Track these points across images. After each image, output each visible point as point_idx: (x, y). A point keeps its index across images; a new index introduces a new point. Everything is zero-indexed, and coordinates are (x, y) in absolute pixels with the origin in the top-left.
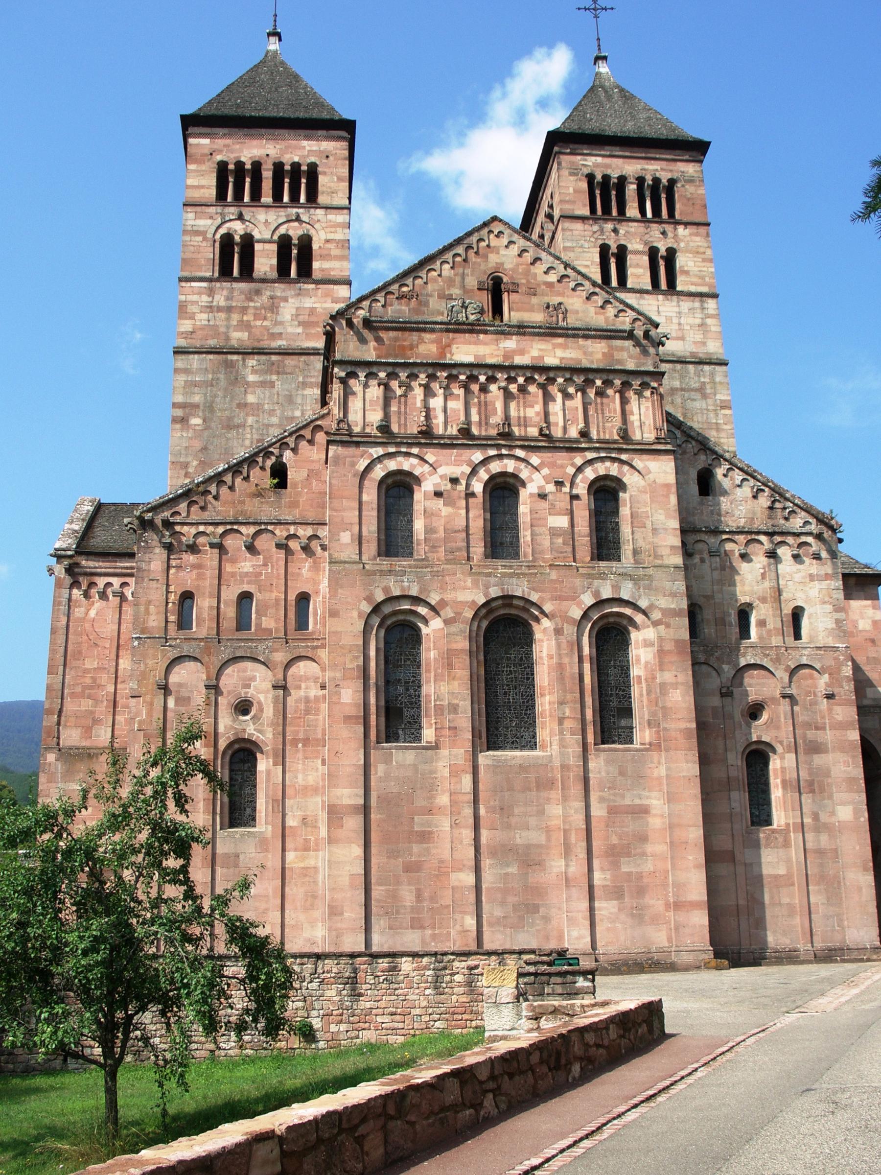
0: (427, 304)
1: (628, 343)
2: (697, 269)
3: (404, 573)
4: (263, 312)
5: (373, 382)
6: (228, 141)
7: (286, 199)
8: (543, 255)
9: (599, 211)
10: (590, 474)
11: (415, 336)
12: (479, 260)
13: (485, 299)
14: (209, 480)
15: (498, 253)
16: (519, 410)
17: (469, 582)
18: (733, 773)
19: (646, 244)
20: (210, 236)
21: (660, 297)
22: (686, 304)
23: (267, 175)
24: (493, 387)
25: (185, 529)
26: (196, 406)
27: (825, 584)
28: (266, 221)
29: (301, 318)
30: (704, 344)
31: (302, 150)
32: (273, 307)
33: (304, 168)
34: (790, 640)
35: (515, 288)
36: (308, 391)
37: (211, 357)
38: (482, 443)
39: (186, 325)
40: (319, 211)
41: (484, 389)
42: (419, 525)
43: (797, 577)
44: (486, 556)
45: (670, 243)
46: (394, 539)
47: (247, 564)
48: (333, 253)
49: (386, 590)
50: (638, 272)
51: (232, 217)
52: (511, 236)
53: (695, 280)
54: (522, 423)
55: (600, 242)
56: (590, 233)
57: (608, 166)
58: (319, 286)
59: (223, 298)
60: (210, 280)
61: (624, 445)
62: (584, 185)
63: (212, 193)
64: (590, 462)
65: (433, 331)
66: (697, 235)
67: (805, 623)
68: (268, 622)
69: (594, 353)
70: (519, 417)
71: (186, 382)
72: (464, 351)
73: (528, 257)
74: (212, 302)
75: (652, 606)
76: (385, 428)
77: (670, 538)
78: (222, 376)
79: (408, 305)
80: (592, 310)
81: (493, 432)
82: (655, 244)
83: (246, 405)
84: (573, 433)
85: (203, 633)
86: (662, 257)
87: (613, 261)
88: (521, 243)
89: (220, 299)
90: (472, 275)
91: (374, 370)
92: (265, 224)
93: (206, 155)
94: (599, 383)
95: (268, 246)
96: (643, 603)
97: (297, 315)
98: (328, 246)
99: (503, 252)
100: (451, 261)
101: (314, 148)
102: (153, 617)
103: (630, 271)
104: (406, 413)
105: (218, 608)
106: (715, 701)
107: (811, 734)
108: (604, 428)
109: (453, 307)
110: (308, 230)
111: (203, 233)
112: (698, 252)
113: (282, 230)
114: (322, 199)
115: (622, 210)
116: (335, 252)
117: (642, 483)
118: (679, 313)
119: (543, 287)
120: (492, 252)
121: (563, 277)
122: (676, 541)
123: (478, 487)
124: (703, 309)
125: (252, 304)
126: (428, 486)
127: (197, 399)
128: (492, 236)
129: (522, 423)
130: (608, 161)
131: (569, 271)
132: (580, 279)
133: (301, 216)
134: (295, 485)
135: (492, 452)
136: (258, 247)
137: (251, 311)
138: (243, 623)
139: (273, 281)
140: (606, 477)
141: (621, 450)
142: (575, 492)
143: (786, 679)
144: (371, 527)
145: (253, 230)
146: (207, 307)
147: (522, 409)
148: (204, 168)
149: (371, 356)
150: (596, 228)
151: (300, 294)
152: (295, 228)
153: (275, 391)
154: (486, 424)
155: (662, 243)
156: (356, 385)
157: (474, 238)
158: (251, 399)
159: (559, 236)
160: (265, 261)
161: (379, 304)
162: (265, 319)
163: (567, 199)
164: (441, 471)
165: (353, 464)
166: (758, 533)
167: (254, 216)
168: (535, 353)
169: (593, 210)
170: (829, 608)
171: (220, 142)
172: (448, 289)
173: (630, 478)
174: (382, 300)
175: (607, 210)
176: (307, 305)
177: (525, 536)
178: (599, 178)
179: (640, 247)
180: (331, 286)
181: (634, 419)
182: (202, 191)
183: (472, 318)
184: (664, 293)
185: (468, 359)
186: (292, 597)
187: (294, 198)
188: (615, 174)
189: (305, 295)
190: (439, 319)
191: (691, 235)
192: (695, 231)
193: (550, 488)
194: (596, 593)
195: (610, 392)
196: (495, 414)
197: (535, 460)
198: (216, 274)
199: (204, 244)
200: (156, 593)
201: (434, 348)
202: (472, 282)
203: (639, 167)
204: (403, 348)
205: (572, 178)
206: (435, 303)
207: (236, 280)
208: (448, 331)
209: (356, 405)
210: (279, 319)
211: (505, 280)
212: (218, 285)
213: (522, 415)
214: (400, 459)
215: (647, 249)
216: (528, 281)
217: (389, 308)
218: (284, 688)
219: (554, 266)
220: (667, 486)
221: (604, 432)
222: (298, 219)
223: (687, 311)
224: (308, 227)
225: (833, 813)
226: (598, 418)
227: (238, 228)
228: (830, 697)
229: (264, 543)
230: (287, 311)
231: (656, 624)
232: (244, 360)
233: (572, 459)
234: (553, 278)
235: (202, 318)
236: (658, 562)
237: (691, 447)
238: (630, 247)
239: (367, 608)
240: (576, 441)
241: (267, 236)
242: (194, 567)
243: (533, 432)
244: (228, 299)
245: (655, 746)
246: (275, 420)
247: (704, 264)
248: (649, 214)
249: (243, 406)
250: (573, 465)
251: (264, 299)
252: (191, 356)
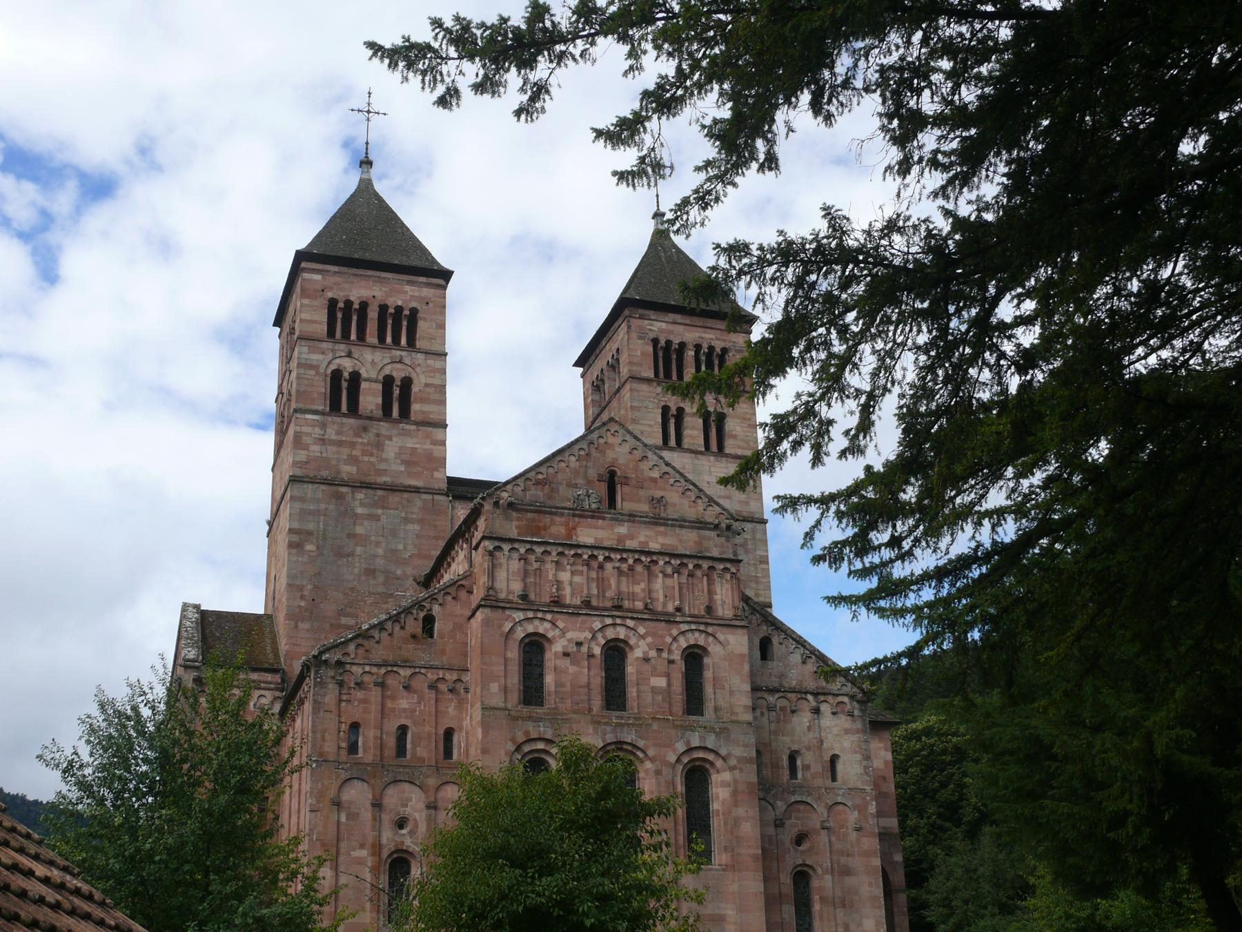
0: (557, 492)
1: (713, 534)
3: (541, 720)
5: (515, 555)
6: (337, 279)
7: (389, 340)
8: (650, 454)
10: (683, 643)
11: (547, 519)
13: (603, 487)
14: (373, 627)
17: (591, 730)
18: (784, 890)
20: (322, 370)
21: (712, 458)
23: (373, 314)
24: (609, 566)
25: (354, 669)
26: (310, 533)
27: (855, 738)
29: (403, 457)
30: (747, 503)
31: (405, 294)
32: (379, 445)
33: (407, 312)
34: (828, 782)
36: (410, 527)
37: (323, 487)
38: (600, 611)
39: (302, 456)
41: (601, 567)
42: (549, 679)
43: (835, 731)
44: (602, 708)
46: (532, 692)
47: (404, 703)
48: (431, 397)
49: (527, 733)
57: (671, 332)
60: (322, 413)
61: (708, 618)
62: (651, 349)
63: (323, 328)
64: (683, 633)
65: (562, 515)
67: (840, 767)
68: (421, 752)
69: (686, 541)
71: (301, 509)
72: (586, 535)
73: (638, 454)
75: (729, 754)
76: (524, 597)
77: (743, 699)
78: (332, 507)
81: (609, 604)
83: (355, 535)
84: (670, 608)
85: (369, 758)
91: (516, 546)
92: (371, 363)
93: (316, 291)
94: (691, 566)
96: (723, 752)
97: (400, 454)
98: (428, 390)
99: (617, 449)
101: (416, 294)
102: (327, 744)
103: (686, 432)
105: (381, 738)
106: (771, 830)
107: (843, 860)
111: (314, 367)
113: (387, 371)
116: (434, 396)
117: (723, 652)
122: (748, 702)
123: (597, 651)
125: (360, 440)
126: (558, 647)
127: (311, 526)
130: (671, 327)
131: (668, 469)
134: (441, 636)
135: (609, 621)
136: (364, 385)
137: (358, 447)
138: (401, 750)
139: (379, 420)
140: (696, 646)
141: (707, 624)
142: (672, 657)
143: (826, 814)
144: (515, 680)
148: (316, 303)
149: (514, 534)
151: (406, 434)
153: (380, 523)
154: (604, 596)
156: (501, 557)
158: (359, 530)
159: (626, 393)
160: (370, 399)
162: (372, 455)
164: (569, 635)
165: (501, 626)
166: (806, 693)
168: (642, 539)
170: (859, 757)
171: (331, 280)
173: (714, 648)
176: (410, 445)
177: (632, 692)
178: (662, 343)
181: (718, 597)
182: (315, 326)
183: (594, 506)
184: (714, 455)
185: (589, 541)
186: (441, 732)
187: (396, 341)
188: (676, 341)
190: (568, 504)
193: (653, 654)
194: (688, 742)
195: (699, 573)
197: (642, 630)
199: (317, 378)
200: (330, 722)
201: (563, 530)
202: (592, 473)
203: (697, 335)
204: (539, 528)
205: (640, 342)
206: (563, 491)
207: (345, 415)
208: (574, 515)
209: (501, 575)
210: (384, 455)
212: (330, 419)
214: (536, 622)
218: (435, 808)
220: (742, 655)
225: (860, 925)
227: (347, 365)
228: (858, 830)
229: (420, 684)
230: (390, 450)
231: (732, 769)
232: (353, 493)
233: (670, 630)
235: (315, 449)
236: (734, 718)
237: (756, 618)
239: (511, 747)
240: (673, 615)
241: (373, 375)
242: (360, 701)
243: (639, 605)
244: (338, 433)
245: (726, 868)
246: (380, 551)
249: (352, 536)
250: (670, 635)
252: (306, 486)
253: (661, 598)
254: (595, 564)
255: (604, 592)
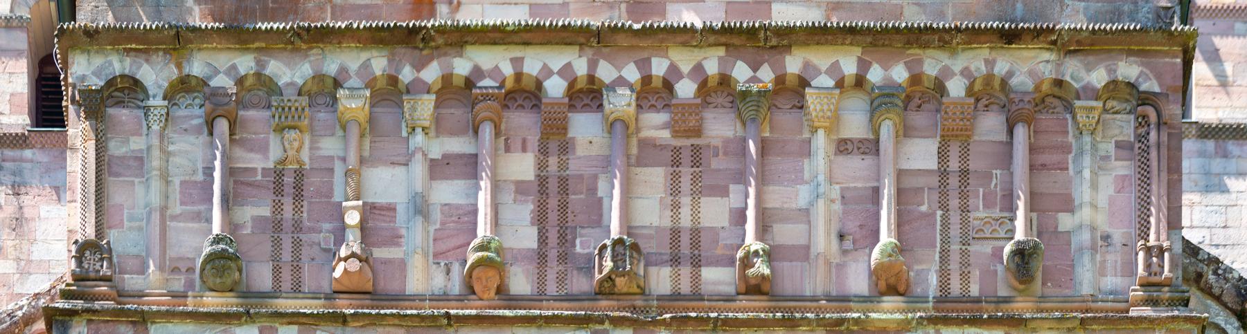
16: (676, 207)
54: (685, 249)
70: (675, 233)
104: (298, 227)
108: (965, 263)
129: (685, 249)
147: (686, 201)
196: (598, 219)
213: (686, 220)
221: (965, 277)
226: (946, 225)
253: (823, 242)
254: (523, 122)
255: (565, 240)
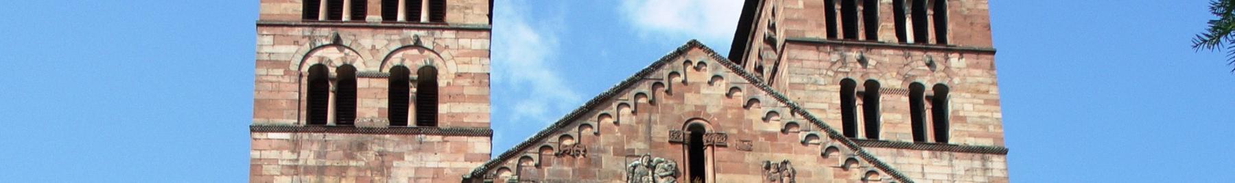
0: (598, 163)
2: (976, 114)
4: (369, 173)
7: (401, 16)
8: (762, 95)
9: (840, 34)
12: (671, 102)
13: (680, 156)
15: (698, 92)
19: (905, 79)
20: (294, 68)
21: (926, 153)
22: (962, 163)
28: (373, 47)
35: (721, 142)
40: (447, 34)
45: (940, 78)
48: (466, 92)
50: (895, 119)
51: (326, 42)
52: (716, 68)
53: (974, 129)
55: (842, 77)
56: (827, 65)
58: (447, 138)
59: (312, 155)
60: (294, 129)
66: (977, 66)
73: (740, 97)
74: (297, 160)
79: (572, 164)
80: (830, 171)
82: (918, 80)
86: (928, 98)
87: (859, 103)
88: (731, 77)
89: (308, 157)
90: (661, 122)
95: (375, 83)
98: (460, 82)
99: (705, 90)
100: (632, 103)
109: (635, 167)
110: (432, 61)
111: (284, 65)
112: (978, 91)
113: (396, 60)
114: (451, 17)
115: (871, 33)
116: (470, 90)
118: (953, 175)
119: (761, 139)
120: (690, 91)
121: (790, 125)
124: (985, 169)
125: (352, 163)
128: (689, 68)
131: (798, 118)
132: (813, 129)
133: (422, 40)
136: (361, 83)
137: (352, 173)
139: (383, 131)
145: (354, 60)
146: (290, 167)
150: (835, 57)
151: (420, 148)
152: (413, 58)
155: (928, 78)
157: (665, 72)
159: (784, 68)
160: (372, 103)
161: (531, 163)
163: (795, 16)
167: (356, 40)
169: (831, 31)
172: (628, 142)
174: (536, 158)
175: (850, 32)
179: (898, 84)
180: (465, 138)
184: (931, 148)
189: (427, 151)
191: (968, 66)
192: (975, 61)
198: (303, 122)
199: (287, 79)
202: (661, 132)
207: (331, 129)
211: (708, 130)
212: (305, 136)
215: (907, 87)
216: (740, 131)
217: (546, 169)
219: (777, 109)
222: (418, 45)
223: (962, 172)
224: (433, 55)
227: (334, 58)
234: (775, 126)
238: (883, 84)
241: (375, 68)
244: (319, 155)
247: (986, 107)
248: (910, 38)
251: (370, 156)
